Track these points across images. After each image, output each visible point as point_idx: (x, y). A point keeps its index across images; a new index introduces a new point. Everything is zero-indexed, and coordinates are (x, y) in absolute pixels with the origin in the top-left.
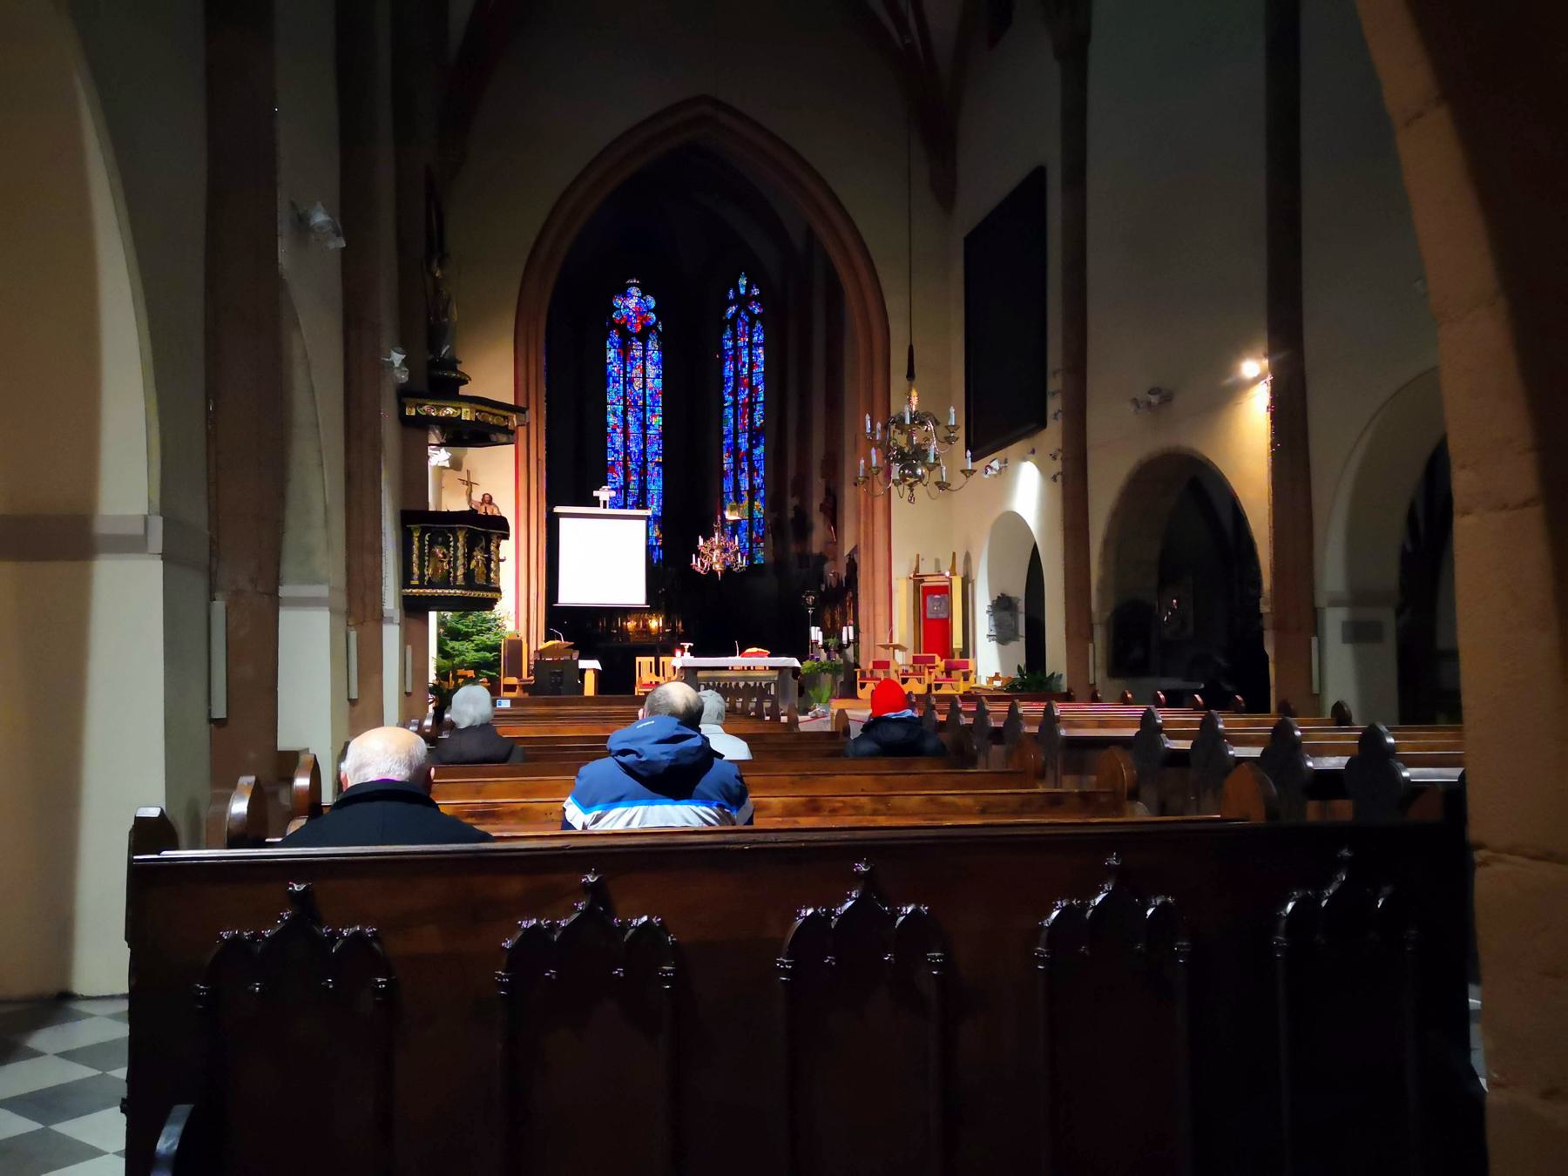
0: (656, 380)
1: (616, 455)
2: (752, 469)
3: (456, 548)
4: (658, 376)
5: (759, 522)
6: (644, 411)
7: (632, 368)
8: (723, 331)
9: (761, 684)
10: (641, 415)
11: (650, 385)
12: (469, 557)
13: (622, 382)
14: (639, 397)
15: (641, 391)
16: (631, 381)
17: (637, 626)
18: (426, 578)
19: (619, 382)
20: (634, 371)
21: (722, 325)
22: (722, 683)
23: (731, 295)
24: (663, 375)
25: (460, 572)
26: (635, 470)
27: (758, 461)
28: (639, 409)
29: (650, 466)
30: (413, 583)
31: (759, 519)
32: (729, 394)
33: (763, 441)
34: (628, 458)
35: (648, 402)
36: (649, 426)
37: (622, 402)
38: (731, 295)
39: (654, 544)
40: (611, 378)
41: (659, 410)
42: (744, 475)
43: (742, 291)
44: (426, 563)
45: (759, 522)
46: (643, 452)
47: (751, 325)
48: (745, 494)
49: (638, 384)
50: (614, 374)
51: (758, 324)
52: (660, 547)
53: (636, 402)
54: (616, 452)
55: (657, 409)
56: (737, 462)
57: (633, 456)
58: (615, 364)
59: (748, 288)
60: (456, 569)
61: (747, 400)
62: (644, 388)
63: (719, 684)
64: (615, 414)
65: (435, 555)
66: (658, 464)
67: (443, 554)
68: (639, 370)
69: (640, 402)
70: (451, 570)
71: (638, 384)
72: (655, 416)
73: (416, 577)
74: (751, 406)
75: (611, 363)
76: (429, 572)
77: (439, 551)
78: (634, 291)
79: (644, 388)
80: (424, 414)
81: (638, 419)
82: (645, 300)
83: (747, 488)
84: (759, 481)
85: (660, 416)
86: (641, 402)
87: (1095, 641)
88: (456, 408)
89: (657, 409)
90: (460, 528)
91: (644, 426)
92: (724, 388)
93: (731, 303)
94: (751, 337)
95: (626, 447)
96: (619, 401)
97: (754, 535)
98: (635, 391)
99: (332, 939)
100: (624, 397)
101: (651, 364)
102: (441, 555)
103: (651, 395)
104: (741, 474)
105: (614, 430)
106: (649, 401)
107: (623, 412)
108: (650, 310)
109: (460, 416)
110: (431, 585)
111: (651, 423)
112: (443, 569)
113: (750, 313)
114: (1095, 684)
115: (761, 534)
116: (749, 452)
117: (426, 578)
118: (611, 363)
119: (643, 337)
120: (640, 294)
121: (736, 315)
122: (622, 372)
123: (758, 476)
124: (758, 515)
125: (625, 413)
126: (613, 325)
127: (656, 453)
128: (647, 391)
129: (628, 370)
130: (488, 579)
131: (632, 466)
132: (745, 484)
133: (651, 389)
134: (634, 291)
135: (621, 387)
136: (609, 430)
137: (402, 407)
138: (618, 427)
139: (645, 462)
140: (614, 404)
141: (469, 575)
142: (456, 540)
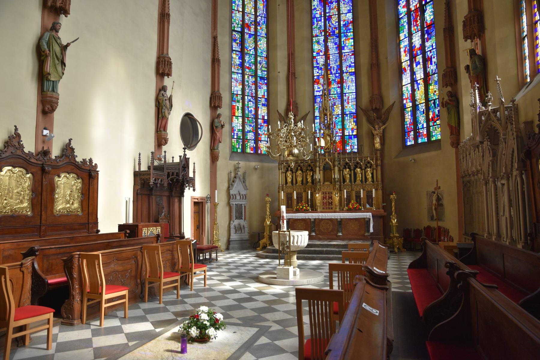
0: (348, 14)
1: (320, 72)
2: (426, 60)
4: (349, 11)
5: (434, 103)
6: (339, 37)
7: (330, 9)
10: (337, 40)
11: (343, 17)
13: (323, 20)
14: (336, 28)
15: (337, 24)
16: (330, 17)
17: (324, 198)
19: (321, 20)
20: (332, 11)
24: (353, 9)
26: (334, 80)
27: (430, 51)
28: (336, 36)
29: (345, 76)
31: (434, 100)
32: (404, 7)
33: (434, 33)
34: (329, 72)
35: (342, 31)
36: (344, 47)
37: (323, 34)
39: (351, 134)
40: (315, 19)
41: (350, 35)
42: (419, 66)
45: (434, 103)
46: (340, 67)
48: (421, 82)
49: (334, 19)
50: (318, 16)
52: (355, 136)
53: (334, 32)
54: (321, 69)
55: (349, 34)
56: (412, 58)
57: (332, 71)
58: (318, 9)
61: (418, 5)
62: (339, 22)
64: (318, 43)
66: (351, 74)
68: (335, 9)
69: (337, 32)
71: (334, 19)
72: (348, 39)
74: (422, 10)
75: (315, 9)
79: (339, 22)
81: (336, 44)
83: (423, 77)
84: (432, 68)
85: (352, 38)
86: (337, 31)
89: (349, 34)
91: (340, 48)
92: (399, 4)
95: (327, 64)
96: (321, 33)
97: (431, 116)
98: (333, 24)
100: (325, 31)
101: (344, 4)
103: (344, 25)
104: (417, 66)
105: (318, 53)
106: (343, 29)
107: (324, 41)
111: (345, 46)
115: (437, 113)
116: (423, 47)
118: (315, 9)
122: (323, 13)
123: (431, 64)
124: (432, 96)
125: (326, 41)
127: (350, 66)
128: (342, 23)
129: (327, 11)
131: (332, 77)
132: (420, 75)
133: (344, 21)
135: (323, 24)
136: (315, 54)
138: (321, 51)
139: (342, 72)
140: (317, 36)
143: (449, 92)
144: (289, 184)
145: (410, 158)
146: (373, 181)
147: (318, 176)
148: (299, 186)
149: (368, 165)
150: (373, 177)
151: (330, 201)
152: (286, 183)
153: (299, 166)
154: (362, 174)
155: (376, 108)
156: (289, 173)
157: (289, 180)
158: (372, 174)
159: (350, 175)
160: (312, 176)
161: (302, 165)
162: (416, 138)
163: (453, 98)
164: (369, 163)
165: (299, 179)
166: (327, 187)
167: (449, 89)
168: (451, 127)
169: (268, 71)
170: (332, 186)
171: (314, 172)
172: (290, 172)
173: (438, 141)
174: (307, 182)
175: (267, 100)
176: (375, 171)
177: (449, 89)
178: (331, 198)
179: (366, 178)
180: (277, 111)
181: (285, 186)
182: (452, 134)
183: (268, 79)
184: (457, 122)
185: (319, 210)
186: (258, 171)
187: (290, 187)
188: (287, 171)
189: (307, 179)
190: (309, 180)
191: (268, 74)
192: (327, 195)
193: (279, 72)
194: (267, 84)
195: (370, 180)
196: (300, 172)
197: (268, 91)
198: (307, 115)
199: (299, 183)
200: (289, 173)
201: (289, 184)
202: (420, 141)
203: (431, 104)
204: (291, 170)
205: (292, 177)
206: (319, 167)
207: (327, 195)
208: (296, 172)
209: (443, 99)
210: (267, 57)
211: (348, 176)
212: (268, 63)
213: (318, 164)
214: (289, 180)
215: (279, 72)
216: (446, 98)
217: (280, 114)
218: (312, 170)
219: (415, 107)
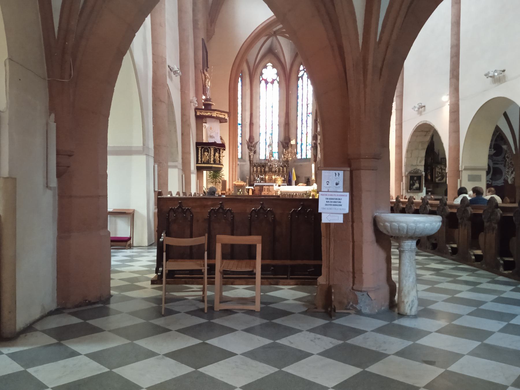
3: (210, 153)
8: (298, 79)
9: (300, 194)
12: (214, 155)
17: (269, 178)
18: (203, 161)
21: (298, 79)
22: (289, 194)
25: (212, 159)
30: (199, 162)
44: (203, 157)
60: (210, 158)
63: (288, 194)
65: (205, 155)
67: (207, 154)
70: (209, 159)
73: (200, 161)
76: (203, 159)
77: (206, 153)
80: (202, 114)
87: (403, 182)
88: (211, 113)
90: (212, 147)
99: (185, 209)
102: (207, 155)
109: (212, 115)
110: (204, 163)
112: (207, 159)
114: (403, 194)
117: (203, 161)
119: (272, 83)
126: (263, 79)
130: (220, 162)
137: (196, 113)
141: (214, 161)
142: (211, 151)
143: (314, 143)
144: (255, 172)
145: (299, 164)
146: (286, 172)
147: (267, 169)
149: (285, 166)
150: (286, 171)
151: (271, 179)
153: (259, 165)
154: (282, 169)
155: (287, 142)
156: (255, 168)
157: (255, 170)
158: (286, 169)
159: (278, 170)
160: (264, 170)
161: (260, 165)
162: (301, 156)
163: (316, 145)
164: (285, 165)
165: (259, 170)
166: (271, 174)
167: (314, 141)
168: (314, 155)
169: (242, 121)
170: (272, 174)
171: (265, 168)
172: (255, 167)
173: (309, 159)
174: (262, 171)
175: (241, 134)
176: (287, 169)
177: (314, 141)
178: (271, 178)
179: (284, 171)
182: (314, 157)
183: (242, 124)
184: (316, 154)
185: (267, 182)
186: (239, 166)
187: (255, 173)
188: (254, 167)
189: (262, 170)
190: (263, 171)
191: (242, 122)
192: (270, 177)
194: (242, 127)
195: (285, 172)
196: (259, 167)
197: (242, 130)
198: (257, 142)
199: (259, 172)
200: (255, 168)
201: (255, 172)
202: (303, 158)
203: (308, 144)
204: (256, 167)
205: (256, 169)
206: (267, 166)
207: (270, 177)
209: (312, 145)
210: (242, 114)
211: (277, 170)
212: (242, 117)
213: (267, 165)
214: (255, 170)
216: (313, 144)
217: (247, 141)
218: (264, 167)
219: (302, 144)
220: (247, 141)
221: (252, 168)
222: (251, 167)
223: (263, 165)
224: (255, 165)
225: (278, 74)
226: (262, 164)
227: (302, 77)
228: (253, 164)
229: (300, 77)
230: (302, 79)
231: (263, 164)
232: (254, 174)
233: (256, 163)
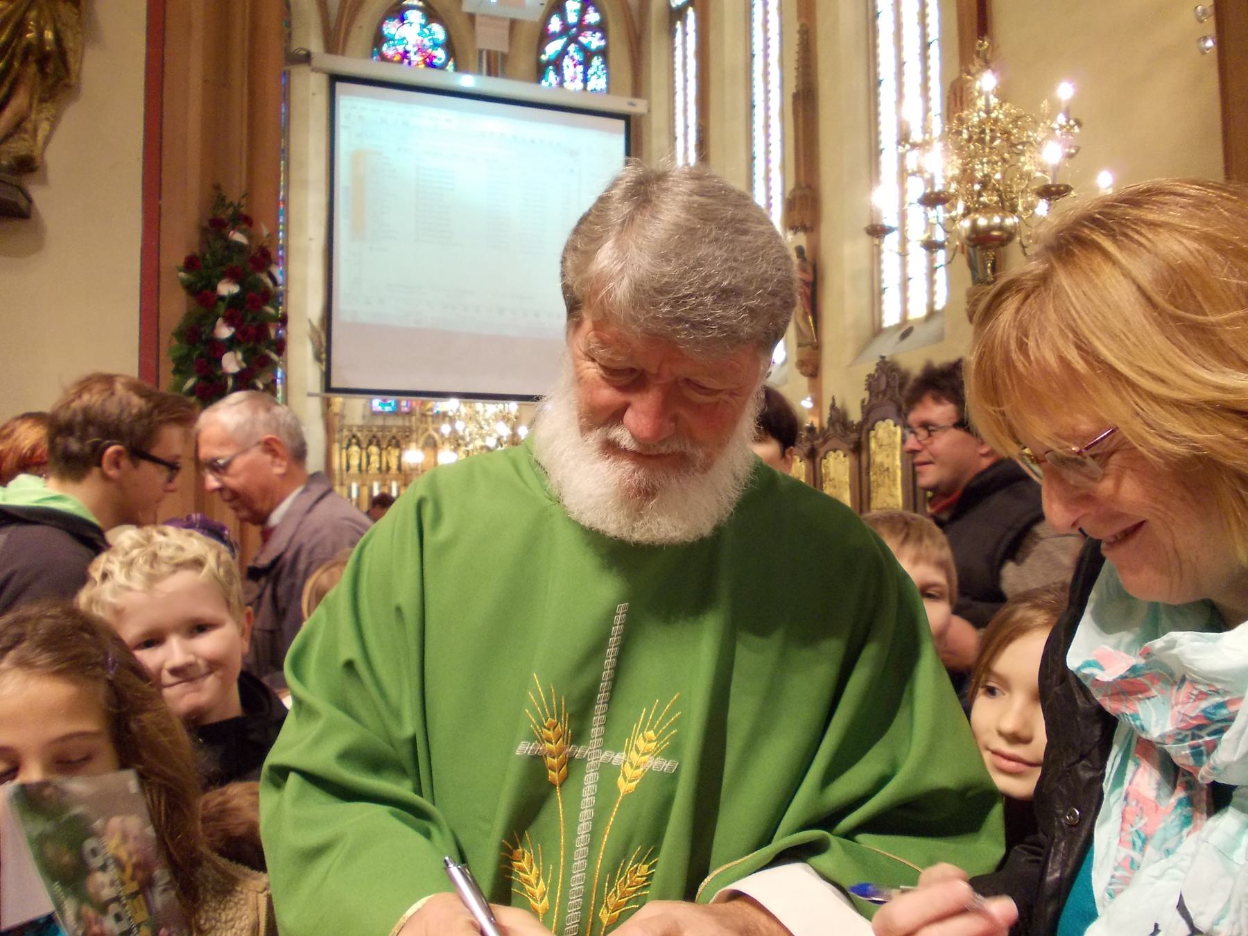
23: (555, 25)
38: (555, 25)
43: (572, 18)
47: (586, 64)
51: (597, 62)
59: (583, 12)
78: (415, 17)
82: (430, 30)
93: (554, 36)
94: (585, 81)
108: (436, 45)
113: (584, 49)
120: (423, 21)
121: (564, 52)
134: (415, 17)
144: (354, 470)
148: (374, 474)
152: (348, 467)
161: (380, 434)
174: (388, 468)
180: (310, 321)
181: (345, 473)
188: (349, 445)
193: (311, 239)
201: (354, 470)
208: (367, 448)
213: (414, 436)
214: (355, 462)
215: (311, 239)
220: (312, 327)
221: (341, 449)
222: (336, 447)
223: (394, 437)
224: (354, 436)
225: (450, 46)
226: (389, 435)
227: (557, 63)
228: (346, 433)
229: (549, 63)
230: (559, 71)
231: (394, 431)
232: (347, 482)
233: (361, 428)
